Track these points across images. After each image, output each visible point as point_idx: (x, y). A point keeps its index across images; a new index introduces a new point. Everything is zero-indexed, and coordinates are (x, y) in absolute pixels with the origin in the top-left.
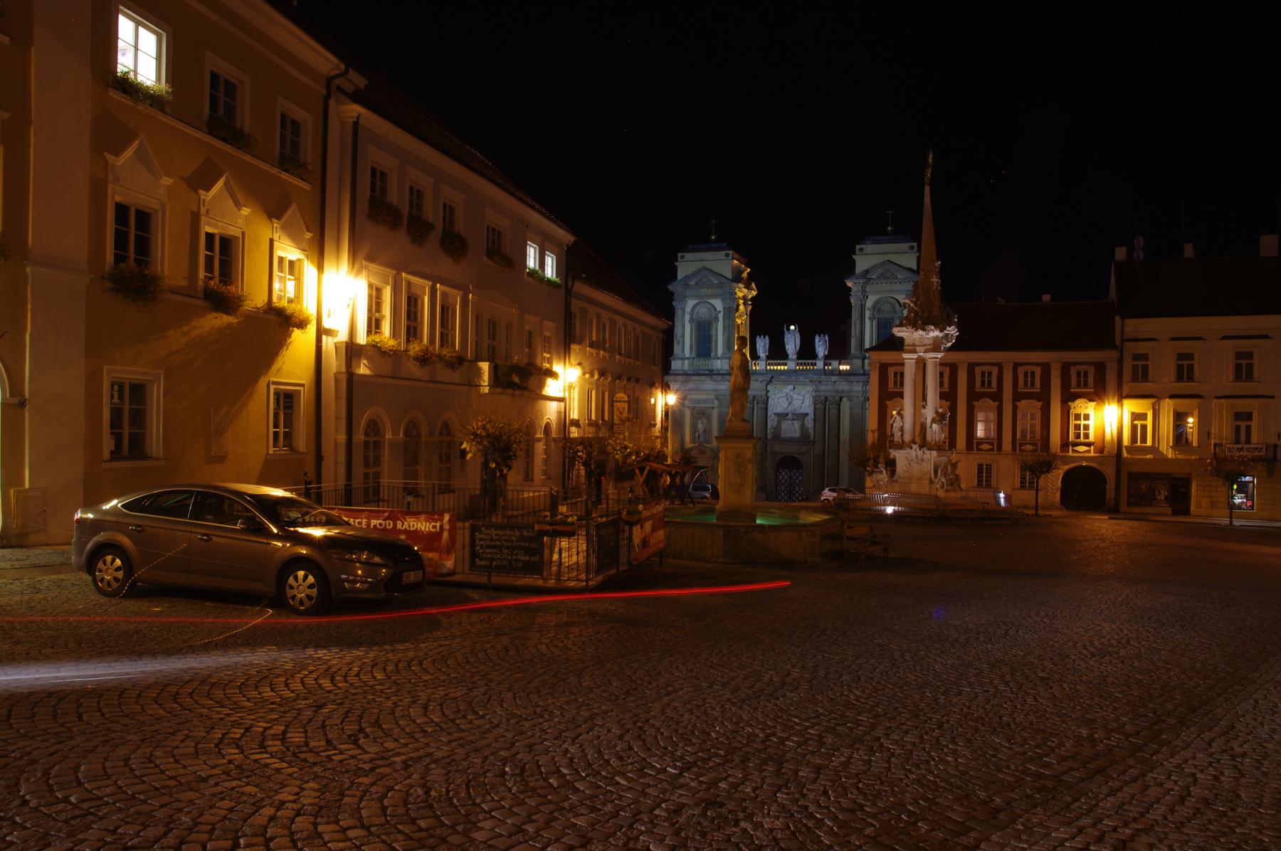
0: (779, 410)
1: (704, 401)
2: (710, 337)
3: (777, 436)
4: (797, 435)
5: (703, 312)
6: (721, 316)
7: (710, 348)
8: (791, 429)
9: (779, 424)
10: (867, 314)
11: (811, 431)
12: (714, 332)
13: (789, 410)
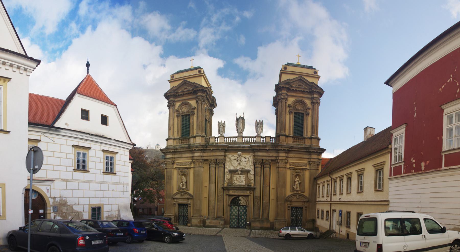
0: (232, 168)
3: (230, 184)
4: (244, 183)
8: (240, 180)
11: (252, 181)
13: (238, 168)
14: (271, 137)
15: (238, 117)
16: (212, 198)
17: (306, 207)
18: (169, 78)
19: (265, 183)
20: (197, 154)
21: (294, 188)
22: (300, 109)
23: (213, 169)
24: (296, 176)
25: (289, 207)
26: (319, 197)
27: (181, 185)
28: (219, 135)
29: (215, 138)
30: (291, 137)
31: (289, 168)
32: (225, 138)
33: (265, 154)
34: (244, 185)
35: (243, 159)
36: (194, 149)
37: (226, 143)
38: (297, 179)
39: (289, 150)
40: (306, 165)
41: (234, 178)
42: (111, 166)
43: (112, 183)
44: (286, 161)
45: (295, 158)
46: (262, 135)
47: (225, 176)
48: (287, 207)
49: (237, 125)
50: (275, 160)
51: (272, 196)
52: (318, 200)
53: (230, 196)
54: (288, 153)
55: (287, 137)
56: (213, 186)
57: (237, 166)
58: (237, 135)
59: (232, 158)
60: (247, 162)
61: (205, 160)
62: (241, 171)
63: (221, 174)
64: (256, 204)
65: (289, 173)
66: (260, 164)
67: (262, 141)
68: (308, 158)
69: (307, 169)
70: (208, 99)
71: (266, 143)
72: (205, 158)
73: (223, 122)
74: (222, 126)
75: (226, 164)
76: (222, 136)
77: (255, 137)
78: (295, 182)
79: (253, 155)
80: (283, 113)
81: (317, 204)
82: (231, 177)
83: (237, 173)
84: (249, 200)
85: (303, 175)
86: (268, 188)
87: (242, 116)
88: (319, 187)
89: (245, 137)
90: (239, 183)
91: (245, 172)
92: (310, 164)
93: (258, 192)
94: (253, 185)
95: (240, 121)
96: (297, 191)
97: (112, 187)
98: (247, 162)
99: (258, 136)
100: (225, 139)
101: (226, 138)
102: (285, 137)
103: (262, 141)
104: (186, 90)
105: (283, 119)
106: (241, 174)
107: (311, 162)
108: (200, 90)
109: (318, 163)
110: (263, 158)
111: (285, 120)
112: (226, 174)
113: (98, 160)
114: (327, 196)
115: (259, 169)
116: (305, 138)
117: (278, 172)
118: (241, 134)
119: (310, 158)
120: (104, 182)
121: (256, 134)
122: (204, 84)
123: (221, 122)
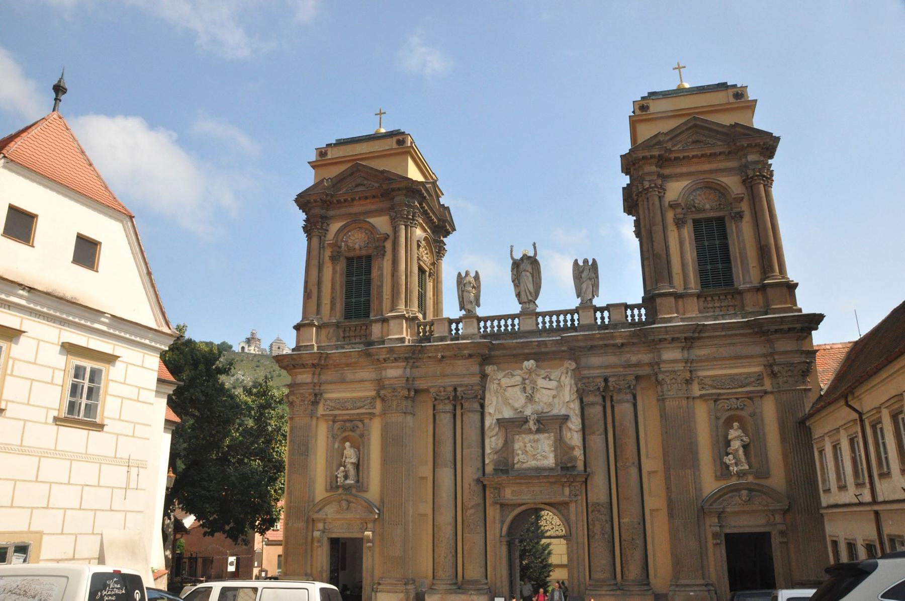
0: (507, 414)
1: (355, 403)
2: (369, 282)
3: (505, 467)
4: (550, 461)
5: (357, 240)
6: (388, 245)
7: (368, 304)
8: (537, 452)
9: (508, 444)
10: (670, 215)
11: (578, 453)
12: (375, 273)
13: (528, 412)
14: (626, 306)
15: (518, 256)
16: (445, 517)
17: (783, 533)
18: (313, 157)
19: (621, 452)
20: (394, 373)
21: (727, 466)
22: (708, 206)
23: (445, 420)
24: (728, 423)
25: (716, 535)
26: (827, 491)
27: (340, 475)
28: (463, 312)
29: (451, 321)
30: (691, 295)
31: (701, 396)
32: (479, 320)
33: (612, 359)
34: (551, 469)
35: (541, 382)
36: (381, 357)
37: (485, 336)
38: (733, 434)
39: (692, 337)
40: (759, 378)
41: (517, 446)
42: (89, 397)
43: (86, 458)
44: (688, 375)
45: (715, 359)
46: (598, 302)
47: (487, 441)
48: (710, 536)
49: (517, 280)
50: (648, 377)
51: (655, 501)
52: (825, 500)
53: (503, 506)
54: (690, 348)
55: (678, 296)
56: (446, 476)
57: (525, 406)
58: (516, 308)
59: (505, 382)
60: (556, 391)
61: (417, 391)
62: (538, 421)
63: (472, 434)
64: (597, 529)
65: (702, 416)
66: (599, 395)
67: (599, 321)
68: (764, 356)
69: (766, 392)
70: (425, 213)
71: (613, 325)
72: (421, 384)
73: (473, 274)
74: (469, 288)
75: (487, 402)
76: (470, 316)
77: (576, 311)
78: (728, 443)
79: (574, 365)
80: (658, 228)
81: (826, 519)
82: (506, 442)
83: (526, 426)
84: (573, 517)
85: (753, 415)
86: (634, 471)
87: (531, 254)
88: (821, 452)
89: (543, 315)
90: (533, 463)
91: (549, 423)
92: (773, 375)
93: (598, 490)
94: (580, 465)
95: (526, 271)
96: (741, 474)
97: (85, 472)
98: (556, 391)
99: (587, 306)
100: (482, 324)
101: (486, 319)
102: (672, 299)
103: (599, 321)
104: (360, 189)
105: (659, 246)
106: (538, 431)
107: (776, 369)
108: (399, 189)
109: (804, 367)
110: (608, 372)
111: (667, 248)
112: (488, 433)
113: (47, 375)
114: (859, 485)
115: (598, 409)
116: (740, 293)
117: (663, 415)
118: (532, 306)
119: (772, 354)
120: (54, 453)
121: (579, 301)
122: (414, 174)
123: (467, 273)
